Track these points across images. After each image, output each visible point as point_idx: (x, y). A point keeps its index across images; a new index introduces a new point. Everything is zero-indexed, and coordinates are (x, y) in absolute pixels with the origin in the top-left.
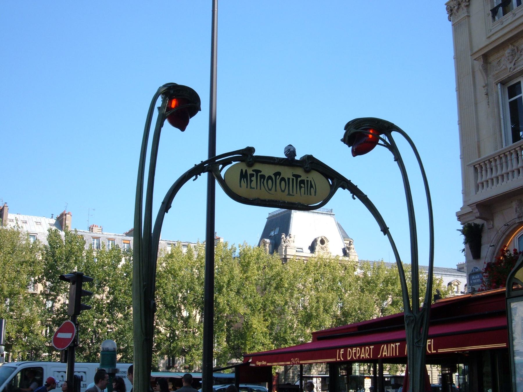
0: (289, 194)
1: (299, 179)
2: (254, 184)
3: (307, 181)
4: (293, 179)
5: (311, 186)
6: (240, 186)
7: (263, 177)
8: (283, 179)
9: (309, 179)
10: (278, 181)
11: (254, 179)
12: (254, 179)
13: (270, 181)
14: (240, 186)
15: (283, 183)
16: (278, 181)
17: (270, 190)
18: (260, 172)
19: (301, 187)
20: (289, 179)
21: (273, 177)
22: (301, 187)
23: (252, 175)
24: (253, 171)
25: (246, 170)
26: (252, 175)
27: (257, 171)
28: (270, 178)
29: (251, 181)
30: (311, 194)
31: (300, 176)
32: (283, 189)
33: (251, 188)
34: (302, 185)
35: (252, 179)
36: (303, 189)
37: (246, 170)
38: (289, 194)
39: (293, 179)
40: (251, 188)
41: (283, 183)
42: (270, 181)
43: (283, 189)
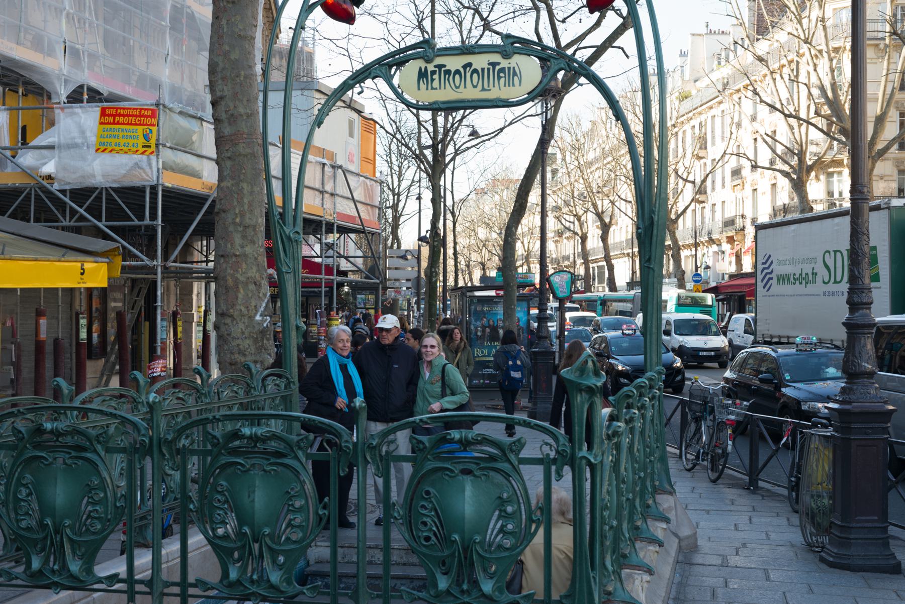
0: (483, 89)
1: (498, 68)
2: (436, 84)
3: (509, 68)
4: (489, 69)
5: (515, 74)
6: (419, 89)
7: (448, 72)
8: (475, 71)
9: (511, 66)
10: (468, 75)
11: (436, 77)
13: (457, 77)
14: (419, 89)
15: (475, 75)
16: (468, 75)
17: (457, 87)
18: (445, 66)
20: (483, 69)
21: (462, 70)
22: (499, 78)
23: (433, 73)
24: (435, 66)
25: (426, 68)
26: (433, 73)
27: (440, 67)
28: (457, 72)
29: (433, 80)
30: (513, 85)
34: (502, 75)
35: (434, 77)
36: (502, 80)
37: (426, 68)
38: (483, 89)
39: (489, 69)
41: (475, 75)
42: (457, 77)
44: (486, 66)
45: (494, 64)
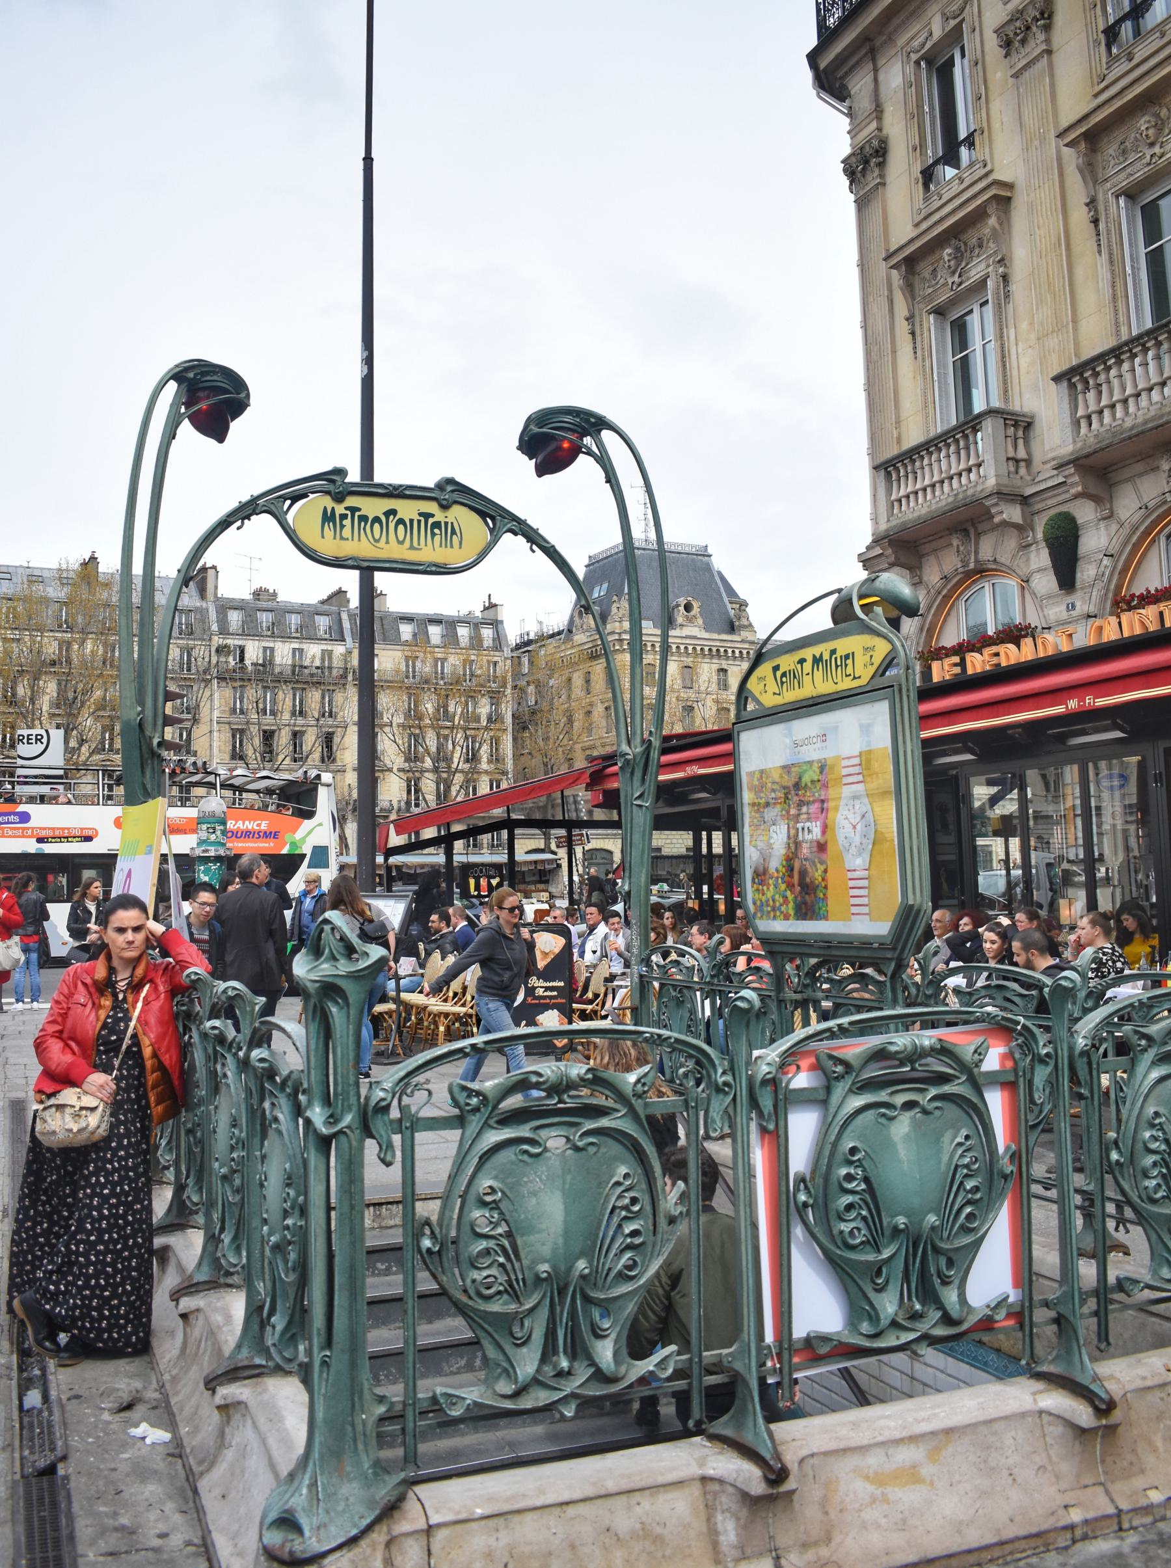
0: (412, 547)
1: (431, 521)
2: (347, 532)
5: (453, 532)
7: (364, 518)
9: (449, 520)
10: (392, 526)
11: (347, 522)
12: (347, 522)
13: (377, 526)
16: (392, 526)
17: (377, 541)
19: (433, 535)
20: (411, 521)
21: (383, 519)
27: (354, 510)
28: (377, 520)
29: (342, 526)
31: (433, 516)
32: (401, 538)
33: (342, 538)
36: (437, 538)
38: (412, 547)
40: (342, 538)
41: (401, 527)
42: (377, 526)
43: (401, 538)
44: (416, 517)
45: (427, 516)
